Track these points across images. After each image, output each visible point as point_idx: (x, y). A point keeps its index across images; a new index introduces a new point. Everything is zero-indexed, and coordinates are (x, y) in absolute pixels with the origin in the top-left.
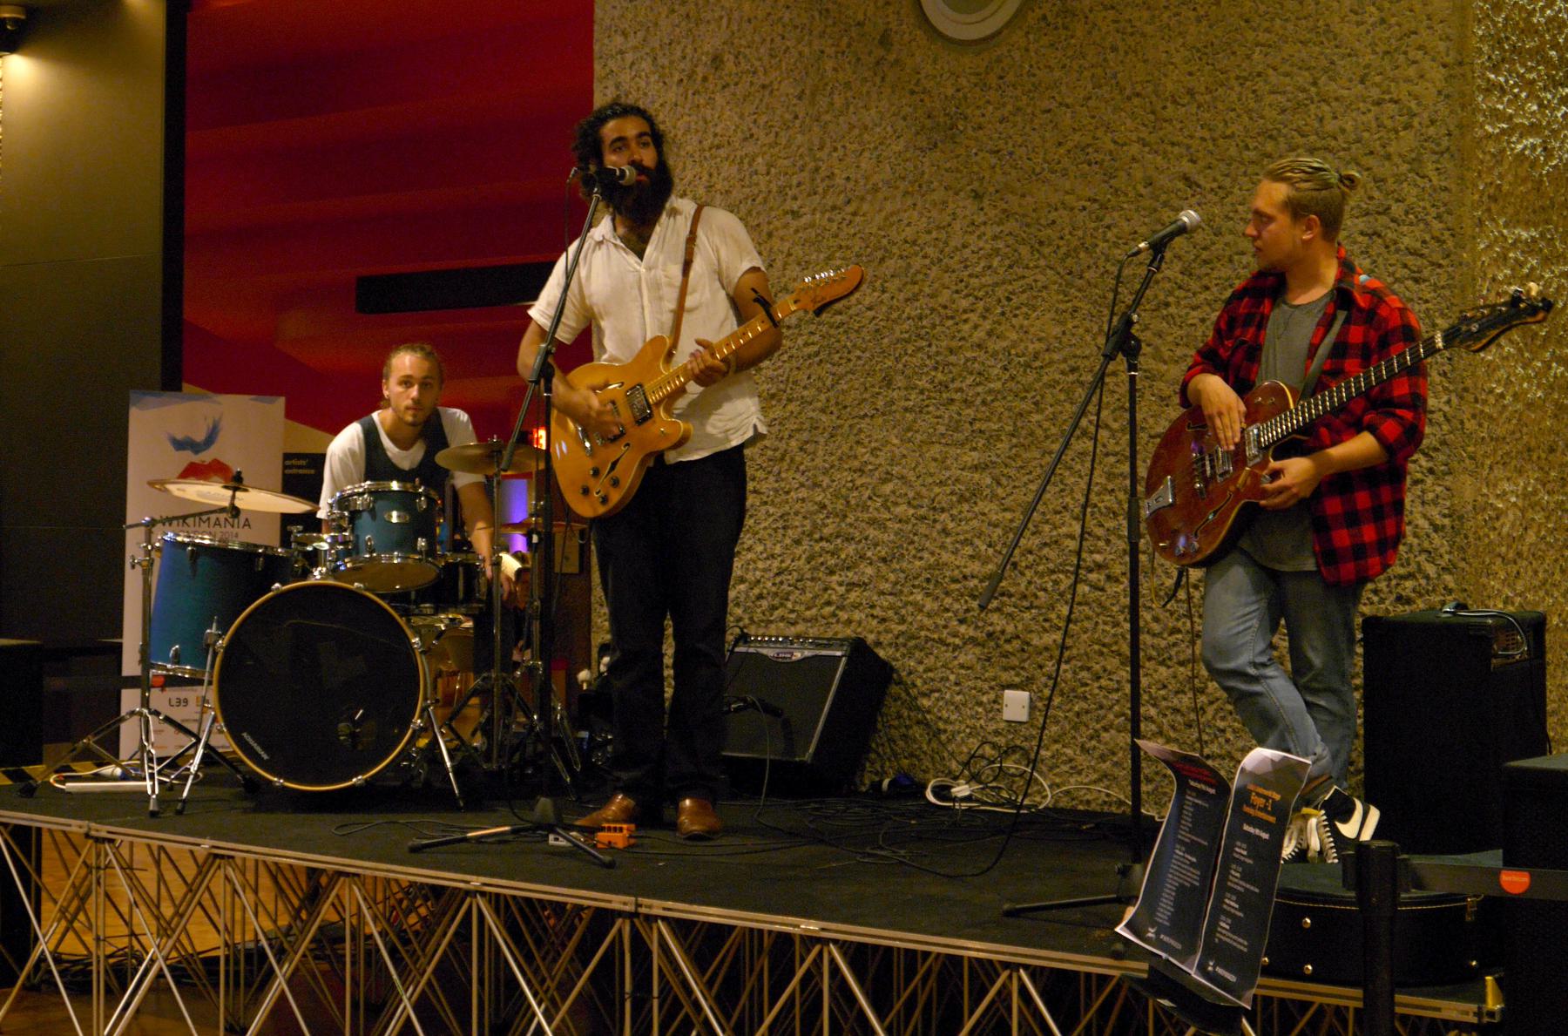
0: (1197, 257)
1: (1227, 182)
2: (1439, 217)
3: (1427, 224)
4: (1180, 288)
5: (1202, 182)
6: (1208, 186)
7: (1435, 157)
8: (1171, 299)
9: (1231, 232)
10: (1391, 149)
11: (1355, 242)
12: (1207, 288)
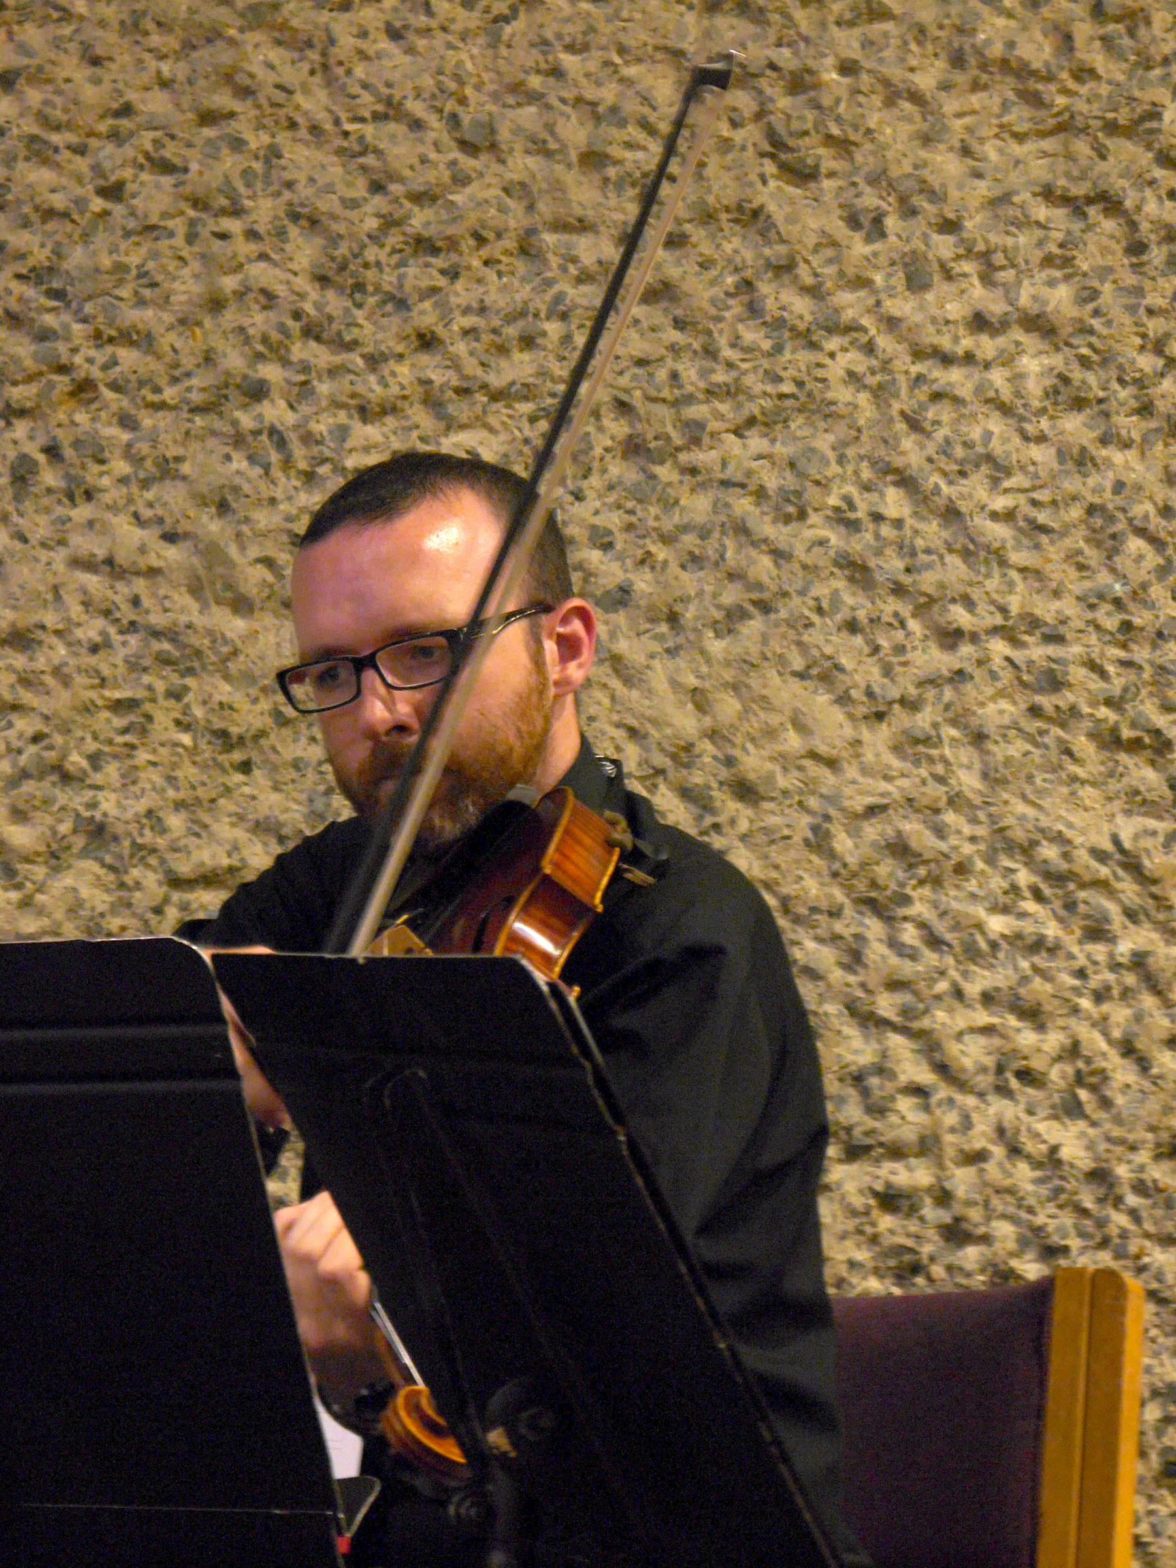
0: (390, 223)
4: (312, 332)
8: (271, 372)
11: (1024, 222)
12: (427, 341)
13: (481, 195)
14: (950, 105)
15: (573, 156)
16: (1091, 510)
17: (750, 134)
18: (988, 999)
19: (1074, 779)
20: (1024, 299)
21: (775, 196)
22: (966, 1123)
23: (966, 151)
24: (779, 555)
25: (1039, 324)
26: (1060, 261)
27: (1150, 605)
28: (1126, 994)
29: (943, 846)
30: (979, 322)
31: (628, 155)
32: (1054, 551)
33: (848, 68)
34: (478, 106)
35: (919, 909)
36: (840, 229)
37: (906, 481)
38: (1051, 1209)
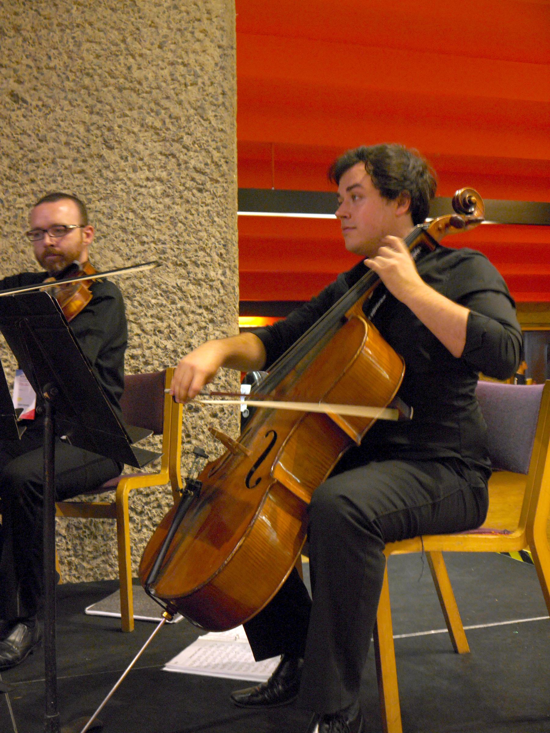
0: (24, 156)
1: (50, 102)
2: (217, 149)
3: (208, 152)
4: (8, 179)
5: (28, 99)
6: (34, 103)
7: (213, 108)
9: (55, 141)
10: (182, 97)
11: (156, 159)
12: (33, 181)
13: (44, 151)
14: (141, 135)
15: (63, 143)
16: (171, 218)
17: (100, 139)
18: (152, 316)
19: (168, 272)
20: (157, 175)
21: (105, 152)
22: (148, 341)
23: (144, 144)
24: (108, 226)
25: (160, 180)
26: (164, 167)
27: (183, 237)
28: (179, 315)
29: (142, 285)
30: (148, 179)
31: (75, 143)
32: (164, 226)
33: (120, 126)
34: (42, 132)
35: (138, 298)
36: (118, 159)
37: (133, 211)
38: (165, 358)
